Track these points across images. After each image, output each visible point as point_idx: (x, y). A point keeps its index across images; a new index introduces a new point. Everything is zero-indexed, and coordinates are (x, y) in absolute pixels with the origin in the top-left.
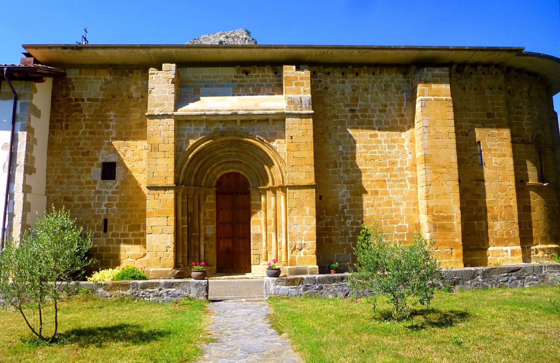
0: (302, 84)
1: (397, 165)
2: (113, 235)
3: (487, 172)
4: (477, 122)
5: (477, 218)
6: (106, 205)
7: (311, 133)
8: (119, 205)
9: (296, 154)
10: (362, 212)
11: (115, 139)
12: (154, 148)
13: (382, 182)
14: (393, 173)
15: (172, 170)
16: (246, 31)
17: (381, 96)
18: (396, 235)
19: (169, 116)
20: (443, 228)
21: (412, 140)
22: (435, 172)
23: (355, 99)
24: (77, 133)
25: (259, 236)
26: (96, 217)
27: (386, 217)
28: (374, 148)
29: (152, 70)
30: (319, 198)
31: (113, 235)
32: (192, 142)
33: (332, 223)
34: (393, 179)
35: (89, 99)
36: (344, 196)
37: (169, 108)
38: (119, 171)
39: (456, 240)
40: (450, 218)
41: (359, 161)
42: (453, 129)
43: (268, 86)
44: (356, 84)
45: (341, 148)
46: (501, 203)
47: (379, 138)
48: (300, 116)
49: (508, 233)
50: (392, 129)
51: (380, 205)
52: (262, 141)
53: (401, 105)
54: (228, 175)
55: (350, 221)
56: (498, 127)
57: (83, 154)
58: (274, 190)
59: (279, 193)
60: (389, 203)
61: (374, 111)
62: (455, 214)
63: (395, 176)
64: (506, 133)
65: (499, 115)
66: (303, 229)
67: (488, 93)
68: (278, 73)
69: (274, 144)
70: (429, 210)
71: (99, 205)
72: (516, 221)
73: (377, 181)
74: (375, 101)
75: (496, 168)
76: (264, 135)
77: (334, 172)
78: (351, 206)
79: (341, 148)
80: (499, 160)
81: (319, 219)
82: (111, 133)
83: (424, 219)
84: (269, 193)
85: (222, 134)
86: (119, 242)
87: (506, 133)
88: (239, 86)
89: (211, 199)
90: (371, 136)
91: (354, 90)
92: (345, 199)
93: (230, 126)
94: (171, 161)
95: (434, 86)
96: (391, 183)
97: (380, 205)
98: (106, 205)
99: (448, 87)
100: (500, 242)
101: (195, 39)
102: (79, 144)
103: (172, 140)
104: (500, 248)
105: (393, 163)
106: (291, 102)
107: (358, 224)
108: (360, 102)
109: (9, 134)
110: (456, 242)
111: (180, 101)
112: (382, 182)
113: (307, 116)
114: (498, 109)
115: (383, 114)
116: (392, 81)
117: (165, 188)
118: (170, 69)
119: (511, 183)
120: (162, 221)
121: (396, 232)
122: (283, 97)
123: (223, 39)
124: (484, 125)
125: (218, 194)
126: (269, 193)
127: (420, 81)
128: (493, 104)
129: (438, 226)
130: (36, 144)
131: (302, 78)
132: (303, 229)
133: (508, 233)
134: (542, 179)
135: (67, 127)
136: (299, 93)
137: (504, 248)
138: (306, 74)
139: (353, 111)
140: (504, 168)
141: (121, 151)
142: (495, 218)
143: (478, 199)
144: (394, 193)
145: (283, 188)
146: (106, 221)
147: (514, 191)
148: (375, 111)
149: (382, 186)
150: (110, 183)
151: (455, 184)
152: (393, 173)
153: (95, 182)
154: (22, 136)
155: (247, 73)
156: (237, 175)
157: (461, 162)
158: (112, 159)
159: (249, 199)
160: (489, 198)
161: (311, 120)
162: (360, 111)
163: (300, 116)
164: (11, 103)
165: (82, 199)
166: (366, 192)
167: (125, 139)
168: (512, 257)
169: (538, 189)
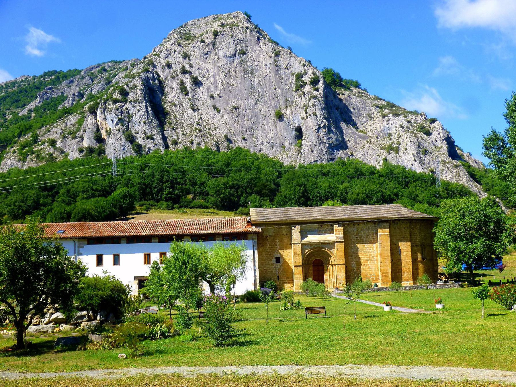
0: (340, 231)
2: (281, 281)
3: (402, 257)
4: (399, 240)
5: (398, 272)
6: (278, 271)
7: (343, 247)
8: (282, 271)
9: (339, 254)
10: (361, 271)
11: (279, 249)
12: (295, 254)
13: (367, 261)
15: (301, 260)
16: (246, 14)
17: (367, 232)
19: (299, 243)
20: (385, 276)
21: (377, 247)
22: (383, 258)
23: (358, 234)
24: (267, 248)
25: (327, 280)
26: (275, 275)
28: (364, 250)
30: (346, 267)
31: (281, 281)
32: (306, 251)
33: (350, 275)
35: (269, 236)
37: (299, 240)
38: (281, 260)
40: (388, 273)
41: (359, 254)
42: (389, 244)
43: (329, 230)
46: (407, 267)
48: (340, 242)
49: (409, 277)
50: (370, 243)
51: (366, 269)
52: (328, 250)
53: (373, 235)
54: (316, 260)
56: (407, 241)
57: (269, 255)
58: (332, 265)
59: (334, 266)
60: (369, 268)
61: (364, 237)
64: (409, 244)
66: (341, 277)
67: (403, 230)
68: (332, 226)
69: (332, 251)
70: (381, 271)
71: (276, 271)
72: (411, 273)
74: (364, 234)
75: (405, 256)
76: (329, 248)
77: (351, 258)
78: (357, 269)
79: (353, 250)
80: (406, 253)
81: (346, 274)
82: (277, 247)
83: (380, 273)
84: (330, 266)
85: (316, 248)
86: (283, 283)
87: (409, 244)
88: (320, 231)
89: (311, 268)
90: (363, 246)
91: (357, 230)
93: (318, 245)
94: (301, 257)
95: (384, 230)
97: (366, 269)
98: (278, 271)
99: (388, 230)
100: (406, 280)
101: (182, 27)
102: (267, 251)
103: (301, 251)
104: (405, 282)
105: (370, 255)
106: (337, 237)
107: (358, 275)
109: (252, 251)
111: (302, 238)
112: (367, 261)
113: (342, 242)
114: (406, 235)
116: (370, 226)
117: (299, 266)
118: (298, 227)
119: (410, 261)
120: (299, 276)
122: (334, 235)
123: (218, 28)
124: (402, 241)
125: (313, 266)
126: (330, 266)
127: (379, 228)
131: (340, 229)
132: (341, 277)
133: (409, 277)
134: (423, 258)
135: (263, 245)
136: (339, 234)
137: (407, 282)
138: (341, 228)
139: (357, 237)
140: (408, 255)
141: (282, 253)
142: (404, 273)
144: (371, 265)
145: (335, 265)
146: (278, 276)
147: (411, 263)
148: (364, 237)
150: (279, 264)
153: (274, 264)
154: (256, 252)
155: (322, 226)
156: (319, 260)
157: (392, 254)
158: (279, 256)
159: (323, 268)
160: (403, 266)
161: (343, 243)
162: (360, 237)
163: (340, 242)
164: (251, 241)
165: (270, 269)
166: (362, 265)
167: (282, 249)
169: (421, 262)
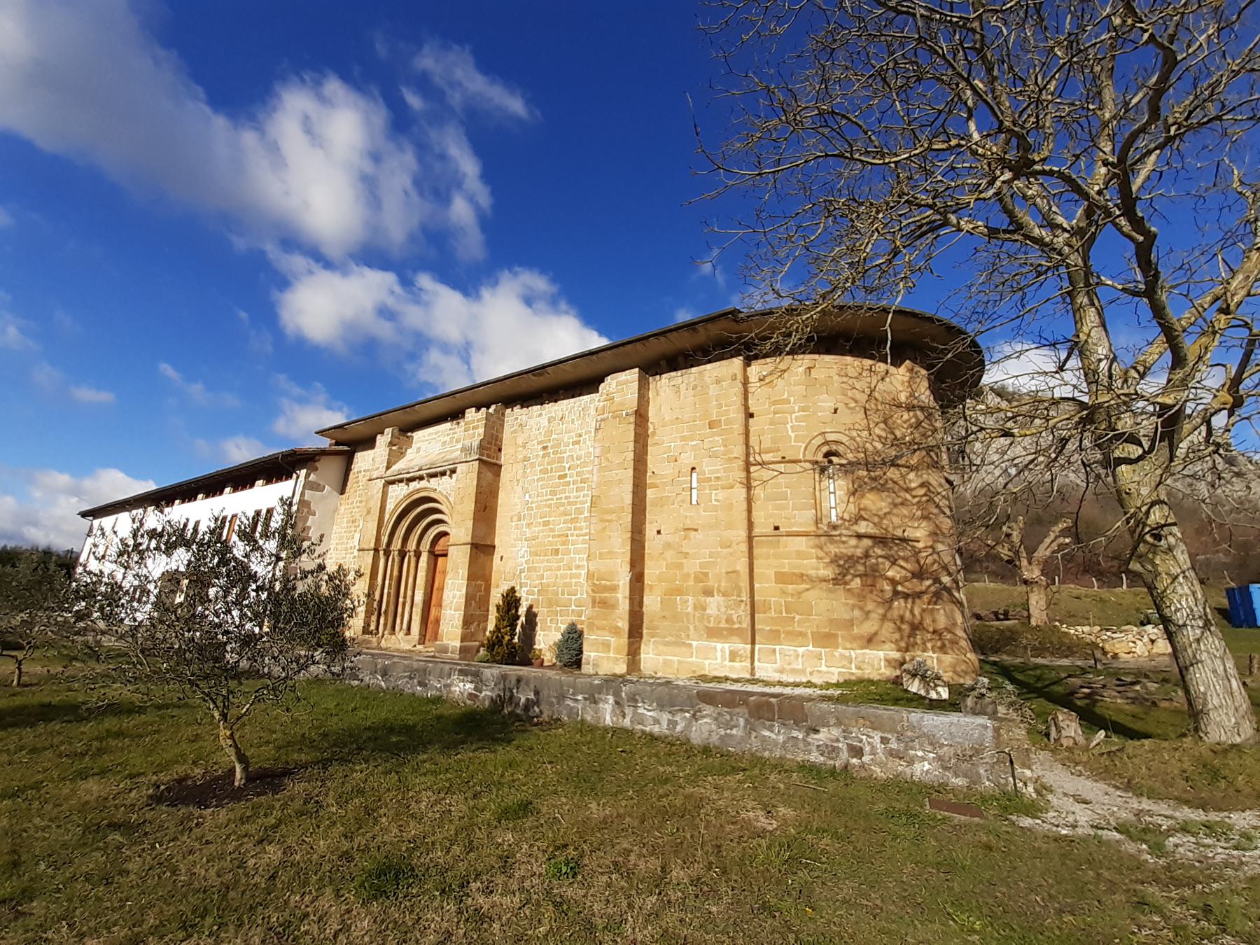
1: (583, 513)
14: (578, 524)
18: (573, 610)
20: (604, 604)
27: (565, 585)
29: (379, 437)
34: (576, 532)
36: (523, 557)
39: (620, 625)
40: (614, 589)
44: (553, 414)
45: (527, 498)
47: (568, 479)
49: (729, 620)
51: (559, 569)
55: (526, 589)
62: (621, 583)
63: (580, 529)
65: (728, 422)
73: (559, 536)
75: (715, 508)
80: (721, 495)
92: (523, 560)
96: (575, 538)
108: (554, 436)
110: (618, 627)
115: (577, 446)
121: (573, 607)
128: (720, 406)
129: (597, 600)
130: (314, 514)
133: (729, 620)
139: (545, 448)
143: (684, 561)
144: (577, 552)
149: (564, 543)
151: (624, 537)
152: (578, 524)
168: (732, 664)
